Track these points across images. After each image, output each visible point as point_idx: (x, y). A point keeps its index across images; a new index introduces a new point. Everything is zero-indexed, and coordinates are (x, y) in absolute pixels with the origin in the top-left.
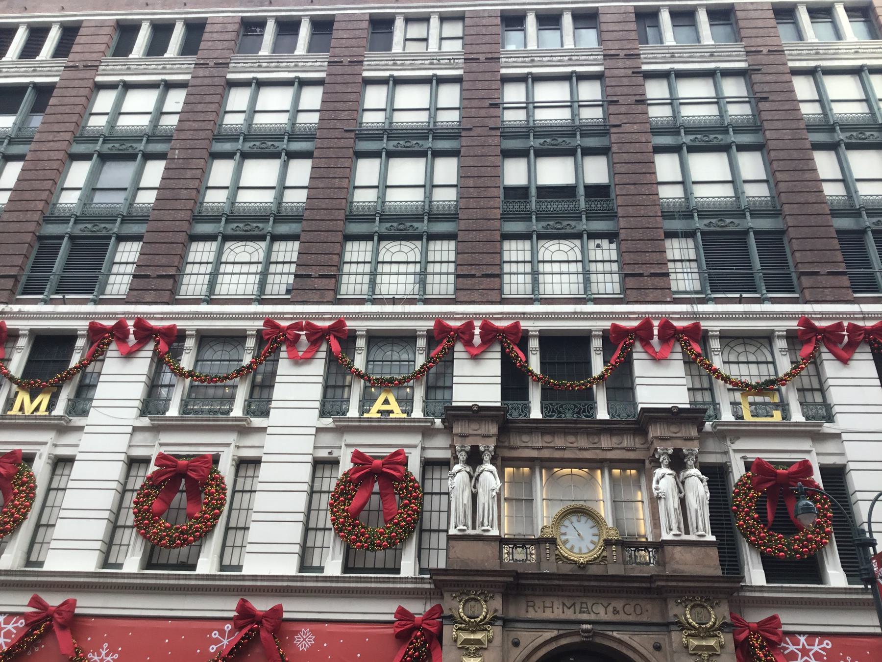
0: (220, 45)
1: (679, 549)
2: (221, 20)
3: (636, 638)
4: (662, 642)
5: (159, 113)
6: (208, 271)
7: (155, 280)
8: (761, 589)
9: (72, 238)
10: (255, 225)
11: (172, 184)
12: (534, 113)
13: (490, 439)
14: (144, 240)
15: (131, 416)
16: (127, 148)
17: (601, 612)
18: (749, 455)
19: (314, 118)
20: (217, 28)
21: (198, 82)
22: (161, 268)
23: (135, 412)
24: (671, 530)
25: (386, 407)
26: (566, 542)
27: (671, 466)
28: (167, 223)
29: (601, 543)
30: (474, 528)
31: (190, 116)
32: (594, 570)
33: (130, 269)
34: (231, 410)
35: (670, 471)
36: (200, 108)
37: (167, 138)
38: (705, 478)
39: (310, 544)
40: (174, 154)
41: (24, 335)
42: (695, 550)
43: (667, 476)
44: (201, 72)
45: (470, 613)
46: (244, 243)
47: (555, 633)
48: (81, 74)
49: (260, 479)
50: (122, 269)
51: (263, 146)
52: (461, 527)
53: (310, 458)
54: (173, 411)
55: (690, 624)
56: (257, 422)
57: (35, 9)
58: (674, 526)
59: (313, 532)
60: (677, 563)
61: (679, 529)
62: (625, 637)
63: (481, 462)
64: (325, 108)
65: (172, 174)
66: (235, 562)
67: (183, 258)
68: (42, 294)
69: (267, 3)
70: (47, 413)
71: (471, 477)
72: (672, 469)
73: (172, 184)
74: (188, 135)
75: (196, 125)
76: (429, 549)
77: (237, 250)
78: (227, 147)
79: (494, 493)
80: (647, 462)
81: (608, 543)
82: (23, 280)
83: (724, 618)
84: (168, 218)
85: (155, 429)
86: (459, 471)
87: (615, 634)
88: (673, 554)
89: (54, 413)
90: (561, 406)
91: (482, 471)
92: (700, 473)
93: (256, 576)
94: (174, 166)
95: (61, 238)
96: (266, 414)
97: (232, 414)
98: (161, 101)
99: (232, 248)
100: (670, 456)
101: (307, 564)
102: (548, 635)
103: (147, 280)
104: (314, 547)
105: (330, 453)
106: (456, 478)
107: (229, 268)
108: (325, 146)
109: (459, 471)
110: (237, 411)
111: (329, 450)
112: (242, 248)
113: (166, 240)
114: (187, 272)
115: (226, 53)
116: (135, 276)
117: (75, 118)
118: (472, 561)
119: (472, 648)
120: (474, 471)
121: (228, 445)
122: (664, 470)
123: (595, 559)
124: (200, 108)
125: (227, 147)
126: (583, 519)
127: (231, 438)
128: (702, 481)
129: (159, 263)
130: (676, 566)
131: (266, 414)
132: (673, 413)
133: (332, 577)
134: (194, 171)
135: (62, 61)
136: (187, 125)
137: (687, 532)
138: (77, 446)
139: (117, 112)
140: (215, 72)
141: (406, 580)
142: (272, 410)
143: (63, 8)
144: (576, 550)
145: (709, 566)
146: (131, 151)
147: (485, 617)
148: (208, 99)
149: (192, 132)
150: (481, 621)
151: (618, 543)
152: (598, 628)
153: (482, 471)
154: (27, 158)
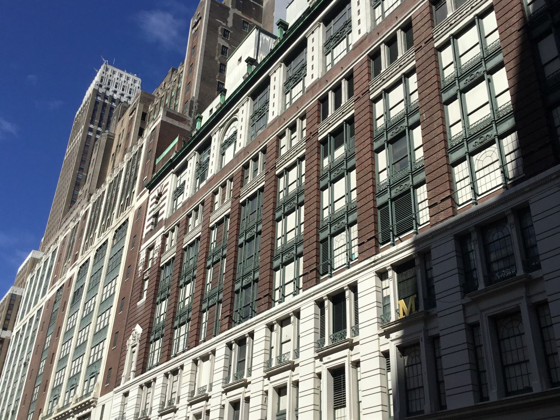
0: (423, 29)
2: (419, 12)
5: (483, 38)
6: (427, 205)
7: (441, 204)
9: (392, 200)
10: (486, 135)
11: (428, 137)
12: (443, 73)
14: (427, 182)
15: (457, 298)
16: (476, 74)
19: (496, 35)
20: (418, 18)
21: (420, 61)
22: (442, 195)
23: (459, 295)
28: (434, 164)
31: (423, 87)
33: (426, 204)
34: (516, 271)
36: (427, 78)
37: (416, 111)
40: (423, 117)
41: (389, 269)
44: (420, 54)
46: (340, 235)
48: (362, 101)
49: (442, 348)
50: (462, 184)
51: (471, 78)
53: (463, 326)
54: (482, 286)
56: (535, 274)
57: (331, 79)
64: (500, 24)
65: (428, 130)
66: (418, 409)
67: (451, 181)
68: (390, 241)
69: (258, 143)
70: (416, 312)
73: (428, 137)
74: (426, 100)
75: (428, 91)
77: (481, 159)
78: (452, 92)
82: (380, 236)
84: (435, 160)
85: (475, 301)
89: (419, 311)
94: (426, 125)
95: (387, 203)
96: (538, 267)
97: (518, 275)
98: (406, 88)
99: (478, 159)
101: (509, 390)
103: (436, 206)
107: (481, 173)
108: (509, 51)
110: (520, 272)
112: (484, 156)
113: (438, 175)
114: (477, 178)
115: (430, 31)
116: (430, 207)
117: (435, 79)
121: (521, 298)
124: (427, 78)
125: (452, 92)
127: (521, 292)
129: (440, 192)
131: (538, 267)
133: (466, 408)
134: (437, 122)
135: (413, 48)
136: (423, 94)
138: (298, 374)
139: (457, 57)
140: (427, 48)
142: (542, 263)
143: (342, 68)
146: (478, 76)
148: (429, 69)
149: (427, 97)
154: (356, 166)
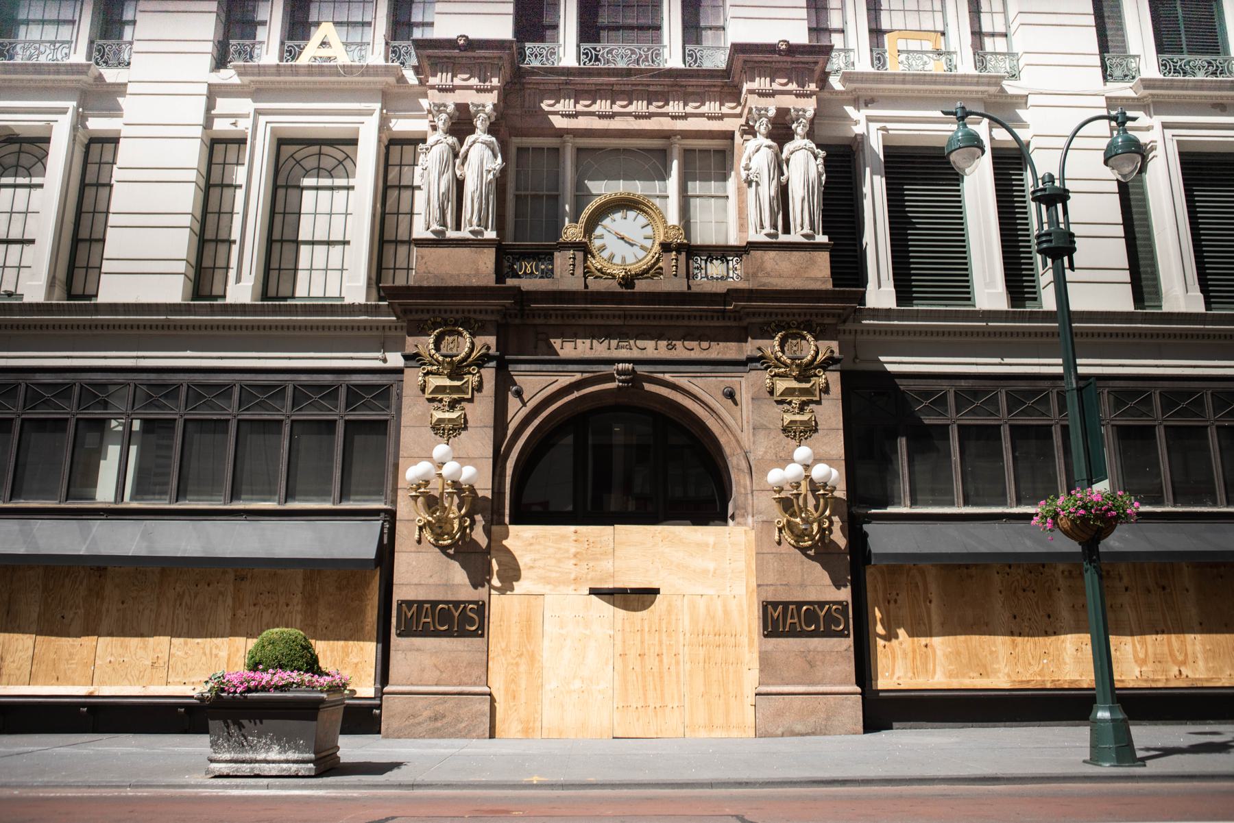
1: (772, 254)
3: (698, 381)
4: (736, 388)
8: (887, 314)
13: (487, 95)
17: (651, 349)
18: (889, 126)
24: (762, 227)
25: (325, 52)
26: (603, 248)
27: (770, 136)
29: (657, 248)
30: (458, 228)
32: (641, 286)
35: (769, 142)
38: (822, 153)
39: (207, 263)
42: (796, 255)
43: (764, 149)
45: (444, 351)
47: (578, 376)
52: (435, 227)
55: (778, 359)
56: (111, 75)
58: (767, 223)
59: (212, 245)
60: (768, 275)
61: (775, 227)
62: (683, 381)
63: (472, 130)
71: (456, 156)
72: (773, 140)
76: (395, 269)
79: (491, 176)
80: (737, 135)
81: (666, 247)
83: (832, 352)
86: (437, 143)
87: (667, 377)
88: (763, 263)
90: (609, 52)
91: (474, 142)
92: (813, 146)
93: (116, 305)
100: (770, 119)
102: (564, 381)
104: (214, 268)
105: (234, 124)
106: (429, 155)
109: (437, 143)
111: (233, 120)
118: (451, 276)
119: (447, 398)
120: (462, 145)
122: (762, 140)
123: (646, 271)
126: (631, 214)
128: (816, 158)
130: (764, 280)
132: (780, 52)
137: (787, 230)
141: (352, 309)
144: (617, 260)
145: (816, 279)
147: (469, 355)
150: (465, 359)
151: (679, 248)
152: (640, 369)
153: (474, 142)
